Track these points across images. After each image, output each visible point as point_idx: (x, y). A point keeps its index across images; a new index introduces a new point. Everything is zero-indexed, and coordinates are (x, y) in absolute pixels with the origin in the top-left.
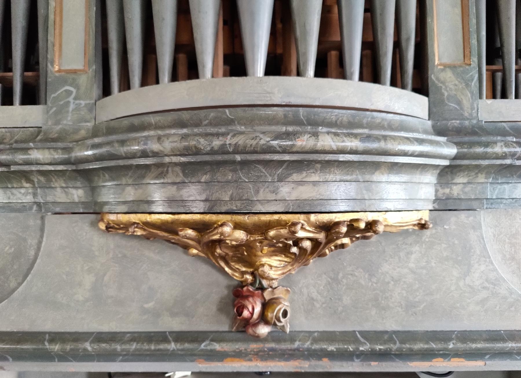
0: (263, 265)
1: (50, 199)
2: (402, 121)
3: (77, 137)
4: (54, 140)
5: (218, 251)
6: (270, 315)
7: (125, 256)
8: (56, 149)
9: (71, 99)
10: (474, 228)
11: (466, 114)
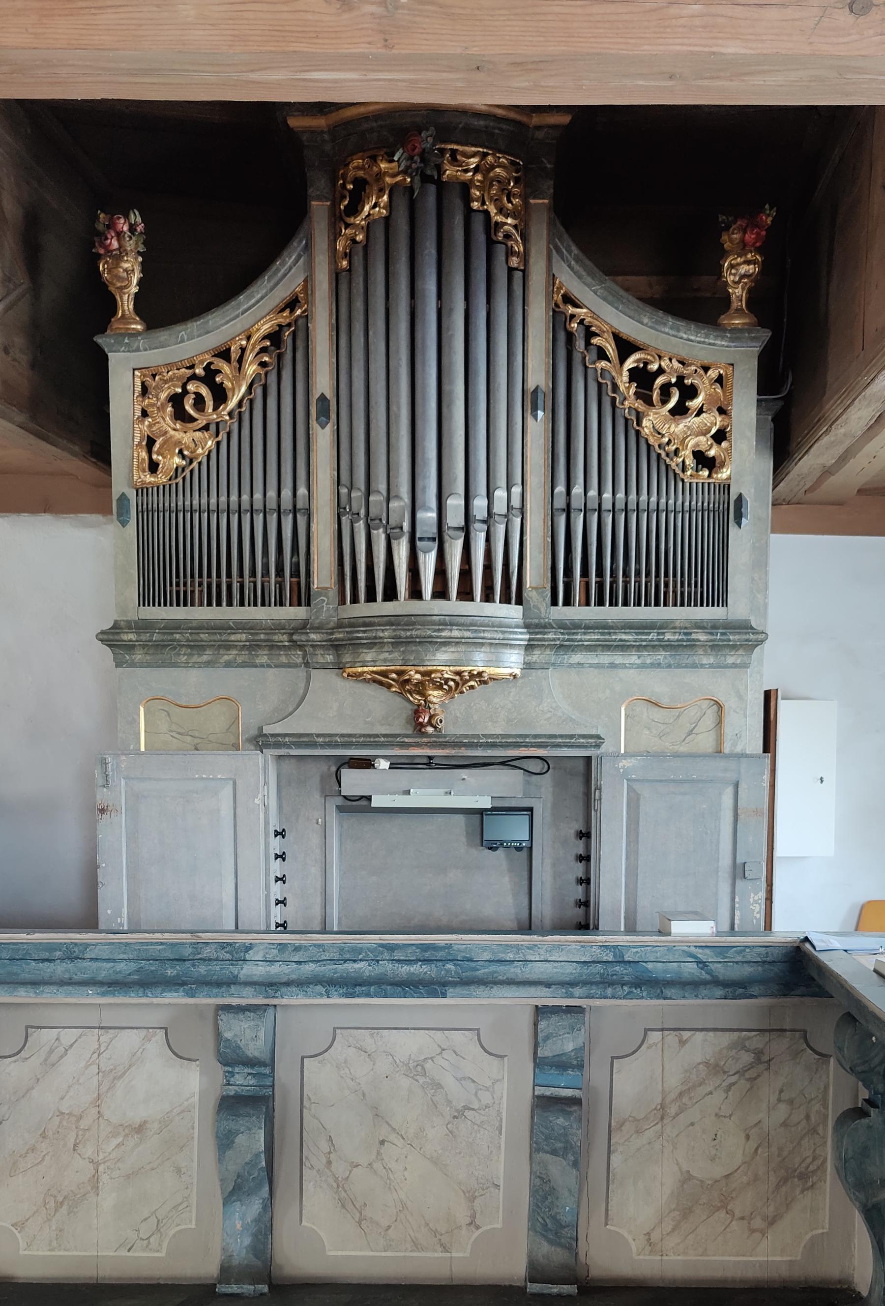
0: (430, 695)
1: (314, 660)
2: (500, 621)
3: (330, 626)
4: (318, 628)
5: (407, 687)
6: (434, 722)
7: (355, 692)
8: (323, 633)
9: (324, 604)
10: (545, 679)
11: (543, 616)
